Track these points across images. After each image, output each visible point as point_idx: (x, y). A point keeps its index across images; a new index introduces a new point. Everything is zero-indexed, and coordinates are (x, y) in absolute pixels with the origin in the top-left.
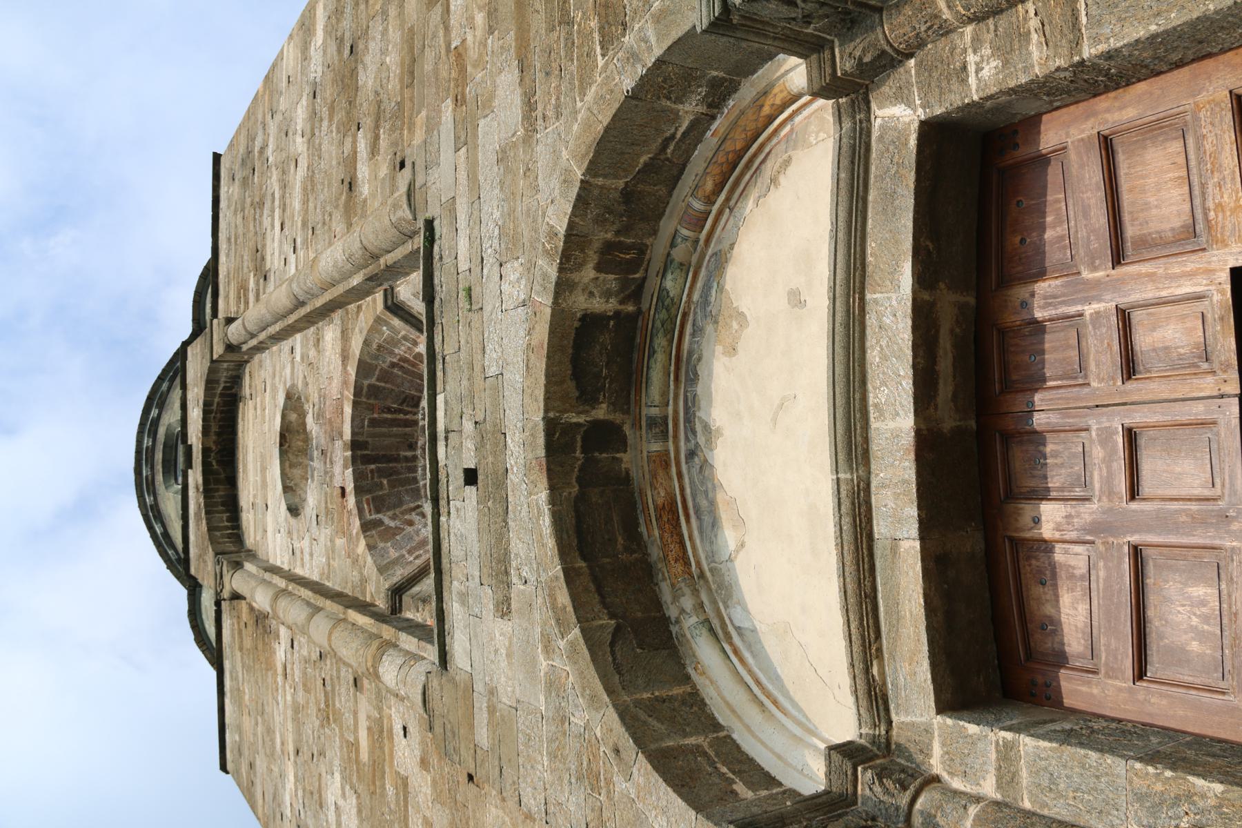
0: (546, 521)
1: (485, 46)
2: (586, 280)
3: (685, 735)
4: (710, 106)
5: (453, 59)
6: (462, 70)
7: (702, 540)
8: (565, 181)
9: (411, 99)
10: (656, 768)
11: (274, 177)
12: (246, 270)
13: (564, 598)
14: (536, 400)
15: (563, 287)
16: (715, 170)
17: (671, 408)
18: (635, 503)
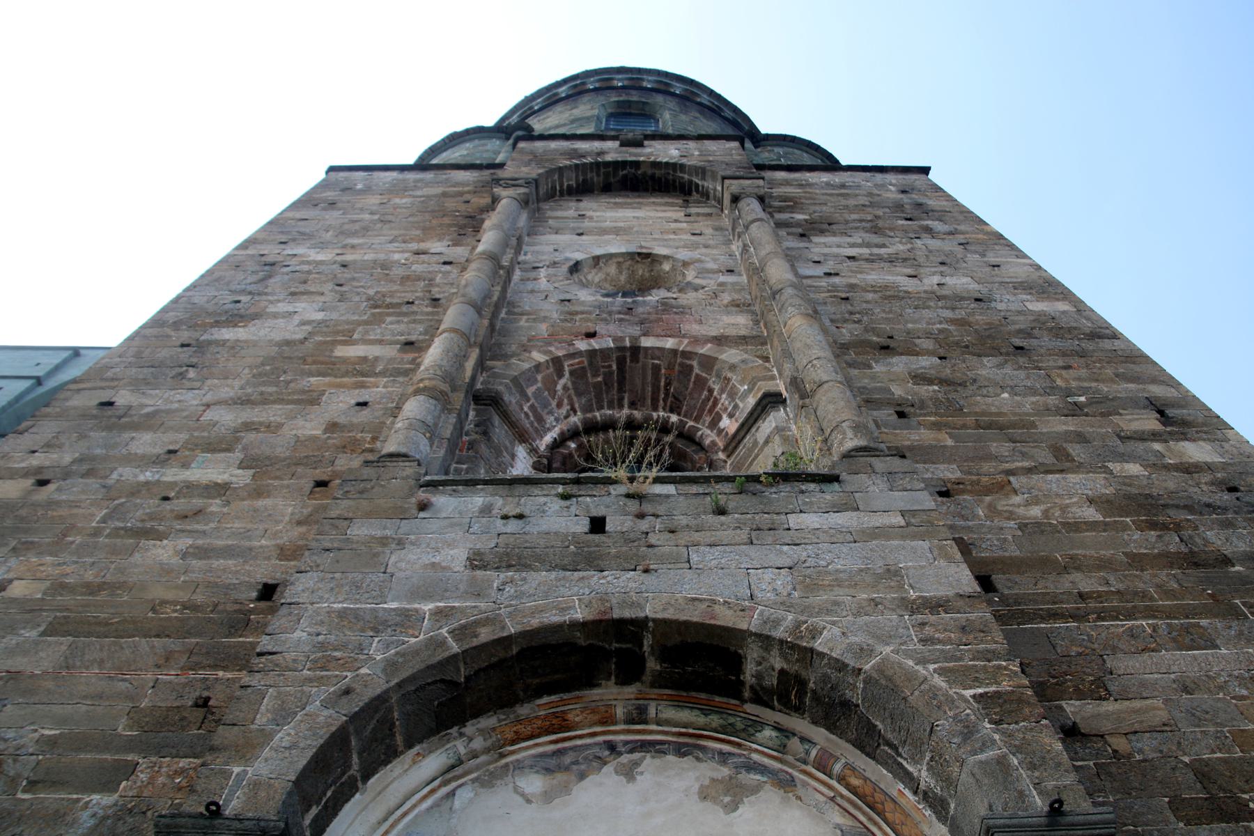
0: (554, 618)
1: (1008, 519)
2: (772, 660)
3: (360, 754)
4: (925, 793)
5: (999, 478)
6: (988, 491)
7: (535, 756)
8: (862, 649)
9: (964, 426)
10: (333, 735)
11: (901, 247)
12: (813, 208)
13: (485, 635)
14: (664, 609)
15: (766, 641)
16: (868, 790)
17: (654, 727)
18: (569, 691)
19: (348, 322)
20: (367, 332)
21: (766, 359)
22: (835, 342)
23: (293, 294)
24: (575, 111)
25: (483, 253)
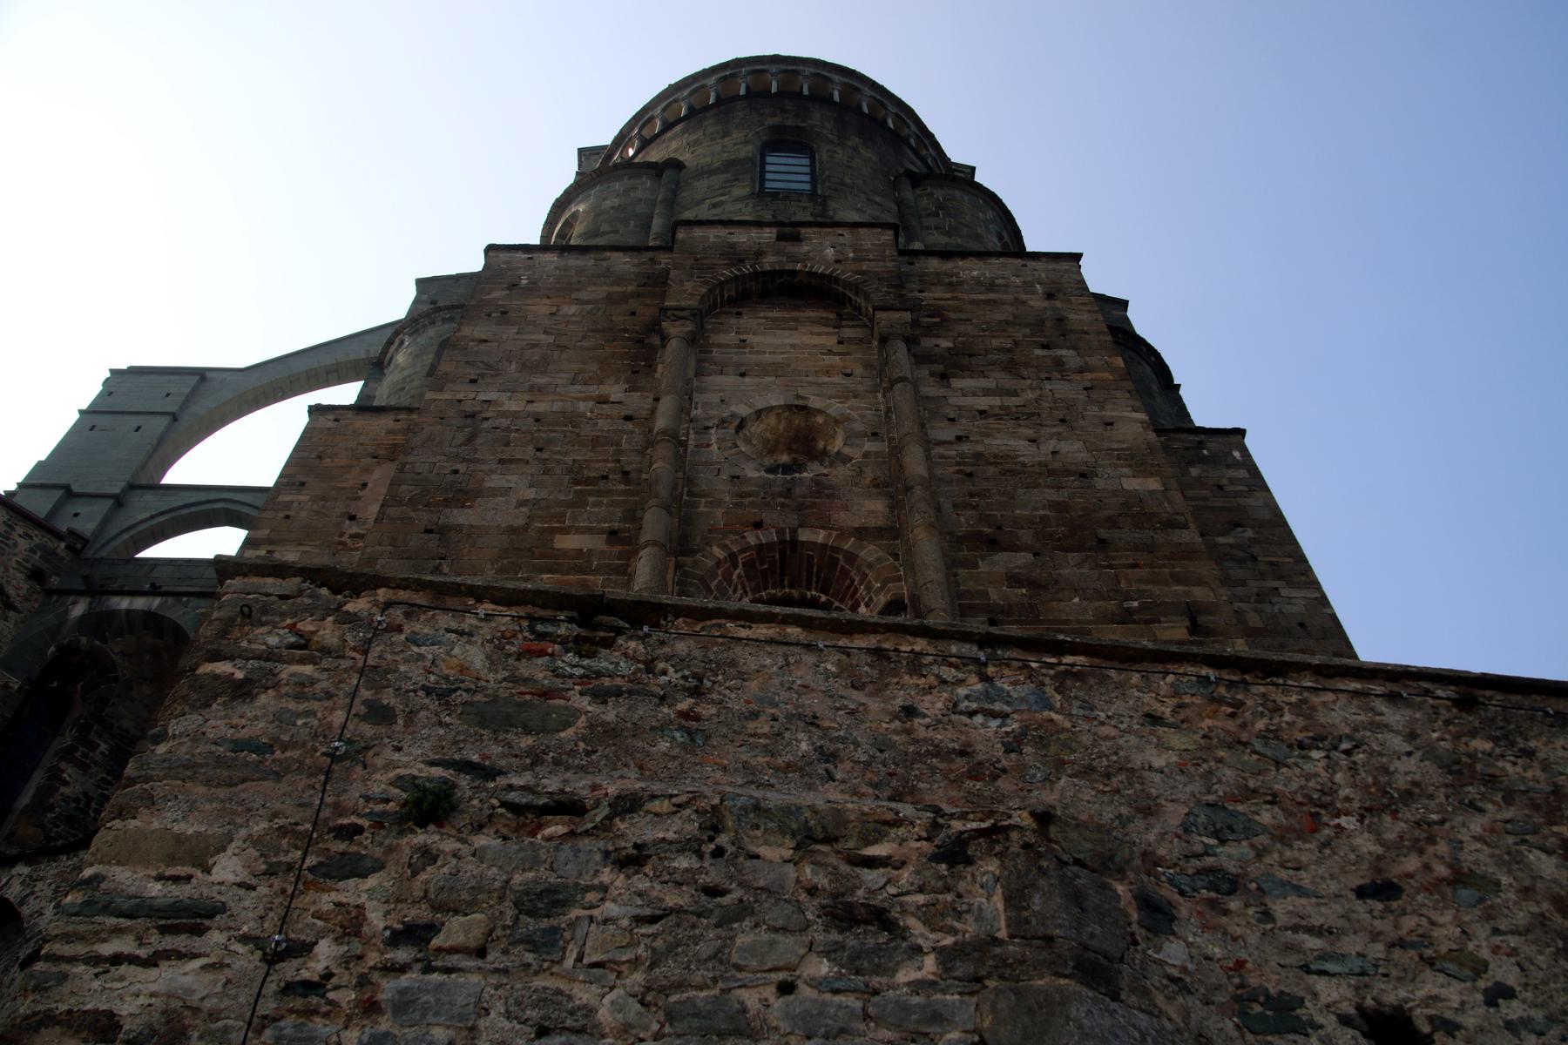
21: (896, 556)
22: (951, 534)
23: (501, 461)
24: (727, 141)
25: (663, 432)
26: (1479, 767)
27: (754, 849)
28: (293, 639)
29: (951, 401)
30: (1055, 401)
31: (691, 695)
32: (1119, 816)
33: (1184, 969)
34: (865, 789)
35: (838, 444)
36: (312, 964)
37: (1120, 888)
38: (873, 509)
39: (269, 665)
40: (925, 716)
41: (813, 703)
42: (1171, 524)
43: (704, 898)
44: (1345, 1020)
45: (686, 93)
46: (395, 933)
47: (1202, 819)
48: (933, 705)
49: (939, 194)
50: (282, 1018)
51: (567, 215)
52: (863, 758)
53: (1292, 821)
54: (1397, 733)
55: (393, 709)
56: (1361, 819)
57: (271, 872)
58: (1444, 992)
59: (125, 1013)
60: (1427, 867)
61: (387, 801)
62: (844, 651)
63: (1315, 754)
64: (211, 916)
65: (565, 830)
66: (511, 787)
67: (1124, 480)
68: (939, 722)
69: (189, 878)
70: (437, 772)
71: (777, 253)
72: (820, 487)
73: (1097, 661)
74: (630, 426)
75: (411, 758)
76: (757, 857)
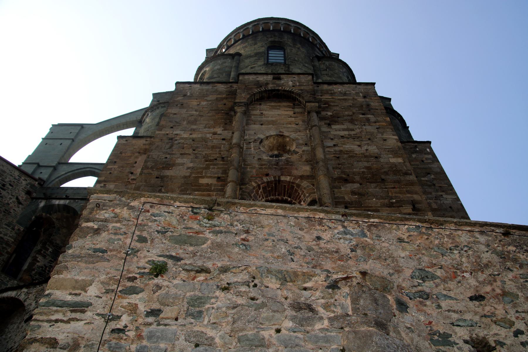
19: (201, 168)
20: (206, 173)
21: (313, 185)
22: (332, 178)
23: (181, 154)
24: (256, 46)
26: (511, 256)
27: (267, 285)
28: (113, 215)
29: (332, 133)
30: (367, 132)
31: (246, 233)
32: (389, 273)
33: (412, 325)
34: (304, 264)
35: (294, 148)
36: (120, 323)
37: (390, 297)
38: (306, 169)
39: (105, 223)
40: (324, 240)
41: (286, 235)
42: (406, 174)
43: (250, 301)
44: (466, 342)
45: (242, 30)
46: (148, 313)
47: (417, 274)
48: (326, 236)
49: (327, 63)
50: (111, 341)
51: (202, 71)
52: (303, 254)
53: (448, 274)
54: (483, 244)
55: (146, 238)
56: (471, 273)
57: (107, 292)
58: (499, 332)
59: (59, 339)
60: (493, 290)
61: (145, 268)
62: (296, 217)
63: (455, 252)
64: (87, 307)
65: (204, 278)
66: (186, 264)
67: (390, 159)
68: (329, 242)
69: (80, 294)
70: (161, 259)
71: (273, 84)
72: (288, 162)
73: (381, 221)
74: (224, 142)
75: (152, 254)
76: (268, 287)
